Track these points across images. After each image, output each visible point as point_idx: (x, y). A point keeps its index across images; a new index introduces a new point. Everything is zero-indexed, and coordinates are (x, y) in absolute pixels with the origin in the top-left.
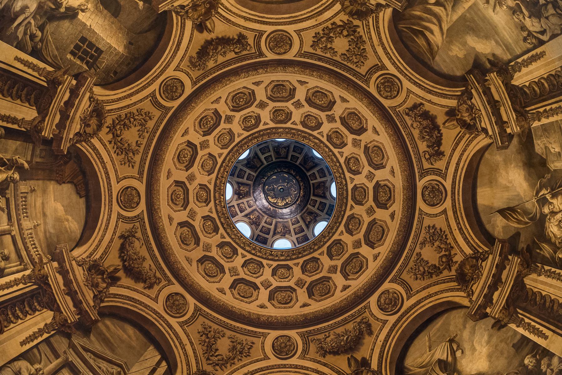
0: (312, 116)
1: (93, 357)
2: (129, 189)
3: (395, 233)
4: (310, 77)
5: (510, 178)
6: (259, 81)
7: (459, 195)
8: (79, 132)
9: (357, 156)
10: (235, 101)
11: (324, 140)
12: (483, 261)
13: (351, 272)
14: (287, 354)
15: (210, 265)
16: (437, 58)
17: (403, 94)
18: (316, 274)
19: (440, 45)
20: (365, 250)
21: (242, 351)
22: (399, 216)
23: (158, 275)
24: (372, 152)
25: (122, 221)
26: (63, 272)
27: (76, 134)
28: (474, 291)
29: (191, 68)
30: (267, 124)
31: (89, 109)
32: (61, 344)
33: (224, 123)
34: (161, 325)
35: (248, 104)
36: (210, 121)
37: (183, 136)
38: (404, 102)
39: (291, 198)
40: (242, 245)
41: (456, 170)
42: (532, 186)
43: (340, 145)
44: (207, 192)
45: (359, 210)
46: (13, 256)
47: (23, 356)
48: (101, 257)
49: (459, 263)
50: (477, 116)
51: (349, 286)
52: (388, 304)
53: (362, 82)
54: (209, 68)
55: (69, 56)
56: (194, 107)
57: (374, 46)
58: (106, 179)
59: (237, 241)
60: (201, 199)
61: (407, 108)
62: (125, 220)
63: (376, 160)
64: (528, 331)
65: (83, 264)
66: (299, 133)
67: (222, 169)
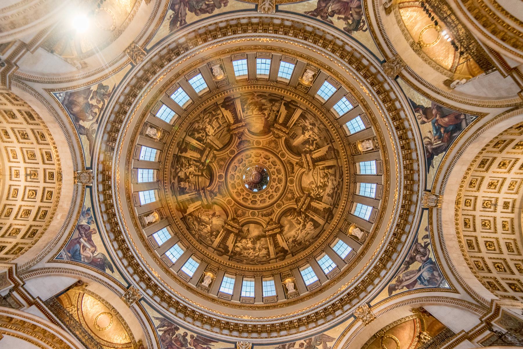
20: (242, 197)
22: (249, 206)
26: (242, 126)
32: (225, 125)
35: (278, 173)
42: (254, 237)
45: (251, 197)
46: (247, 115)
47: (223, 116)
63: (262, 201)
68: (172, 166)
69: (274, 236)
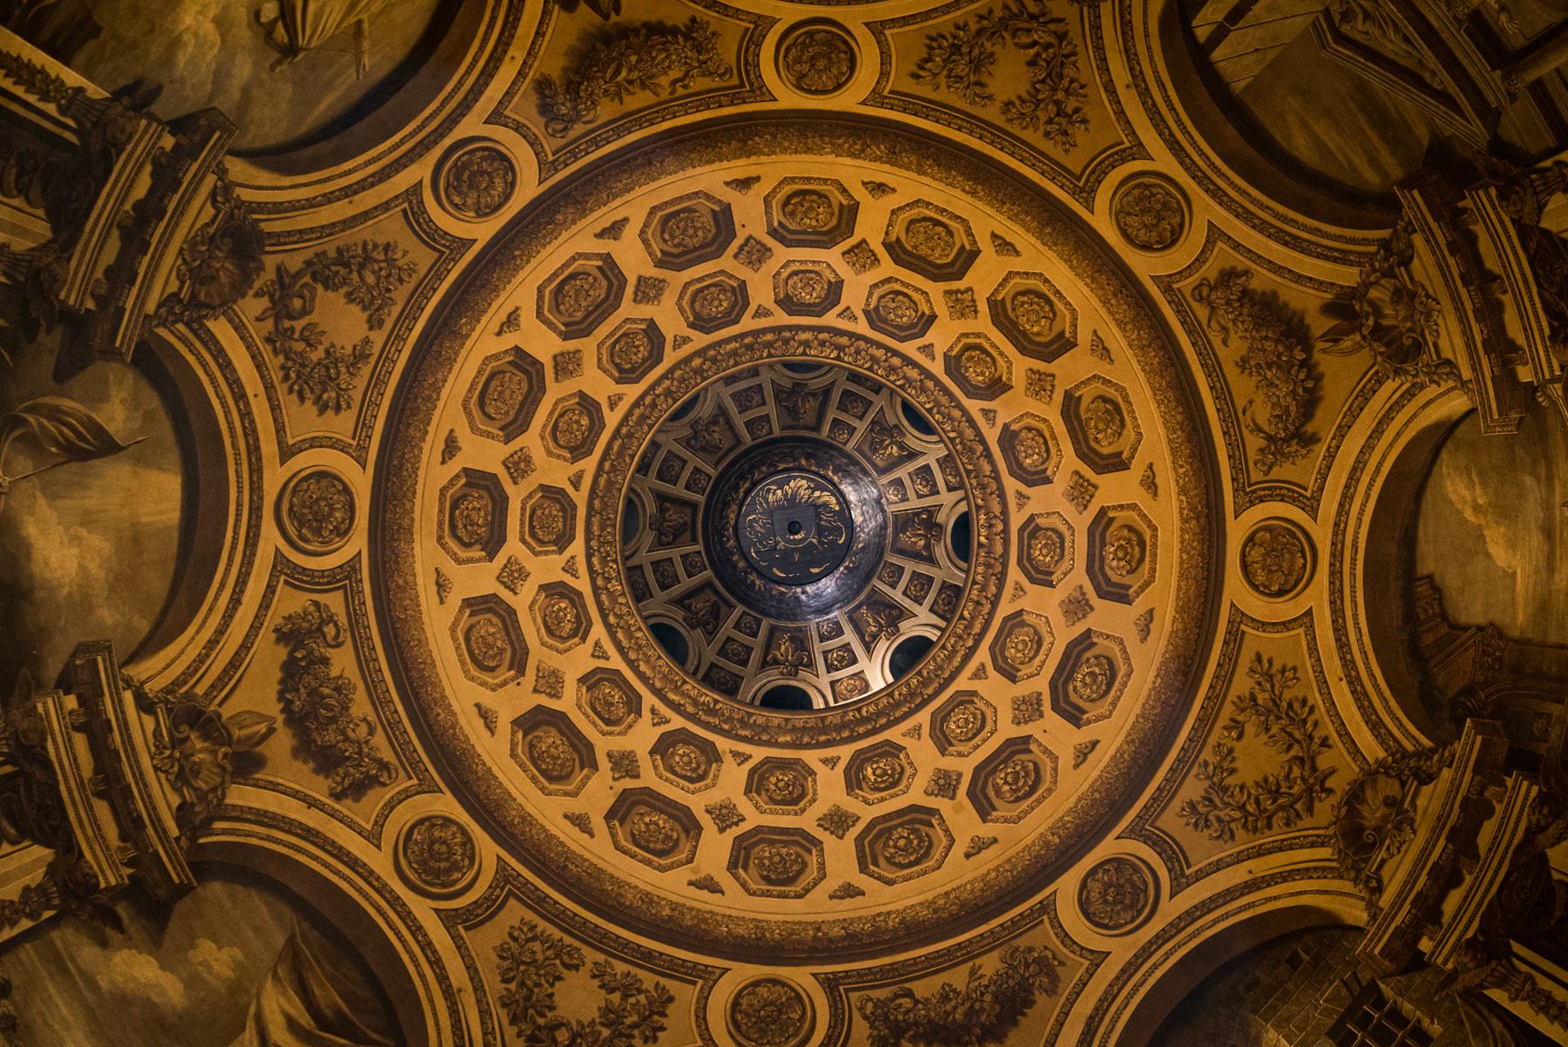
0: (684, 777)
1: (1427, 76)
2: (1275, 588)
3: (444, 393)
4: (682, 900)
5: (75, 551)
6: (842, 898)
7: (239, 504)
8: (1422, 783)
9: (550, 641)
10: (921, 840)
11: (649, 700)
12: (176, 295)
13: (591, 280)
14: (811, 35)
15: (1035, 329)
16: (280, 940)
17: (391, 830)
18: (701, 279)
19: (269, 984)
20: (544, 344)
21: (953, 54)
22: (432, 447)
23: (1202, 312)
24: (502, 651)
25: (1306, 490)
26: (1502, 349)
27: (1430, 778)
28: (209, 204)
29: (1054, 958)
30: (825, 761)
31: (1383, 854)
33: (960, 775)
34: (1202, 154)
35: (880, 830)
36: (1006, 782)
37: (1095, 744)
38: (391, 806)
39: (767, 503)
40: (930, 384)
41: (242, 582)
43: (602, 679)
44: (1030, 560)
45: (554, 471)
48: (1380, 383)
49: (251, 292)
50: (168, 752)
51: (599, 235)
52: (482, 173)
53: (519, 875)
54: (996, 953)
55: (1435, 1029)
56: (1053, 830)
57: (475, 990)
58: (1345, 627)
59: (944, 400)
60: (1049, 538)
61: (384, 785)
62: (1293, 491)
63: (489, 627)
64: (48, 75)
65: (1437, 366)
66: (726, 727)
67: (977, 629)
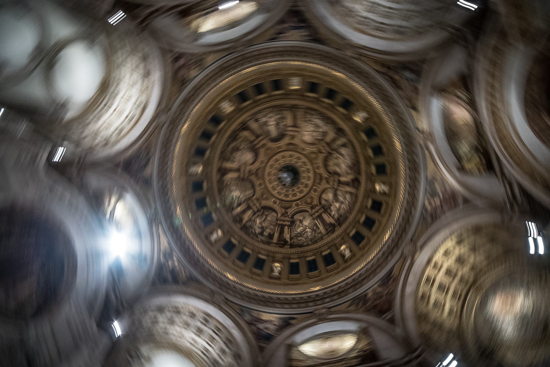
68: (248, 235)
69: (340, 182)
